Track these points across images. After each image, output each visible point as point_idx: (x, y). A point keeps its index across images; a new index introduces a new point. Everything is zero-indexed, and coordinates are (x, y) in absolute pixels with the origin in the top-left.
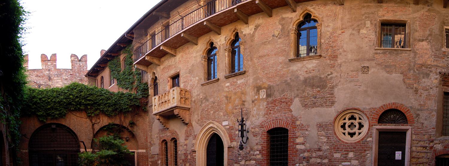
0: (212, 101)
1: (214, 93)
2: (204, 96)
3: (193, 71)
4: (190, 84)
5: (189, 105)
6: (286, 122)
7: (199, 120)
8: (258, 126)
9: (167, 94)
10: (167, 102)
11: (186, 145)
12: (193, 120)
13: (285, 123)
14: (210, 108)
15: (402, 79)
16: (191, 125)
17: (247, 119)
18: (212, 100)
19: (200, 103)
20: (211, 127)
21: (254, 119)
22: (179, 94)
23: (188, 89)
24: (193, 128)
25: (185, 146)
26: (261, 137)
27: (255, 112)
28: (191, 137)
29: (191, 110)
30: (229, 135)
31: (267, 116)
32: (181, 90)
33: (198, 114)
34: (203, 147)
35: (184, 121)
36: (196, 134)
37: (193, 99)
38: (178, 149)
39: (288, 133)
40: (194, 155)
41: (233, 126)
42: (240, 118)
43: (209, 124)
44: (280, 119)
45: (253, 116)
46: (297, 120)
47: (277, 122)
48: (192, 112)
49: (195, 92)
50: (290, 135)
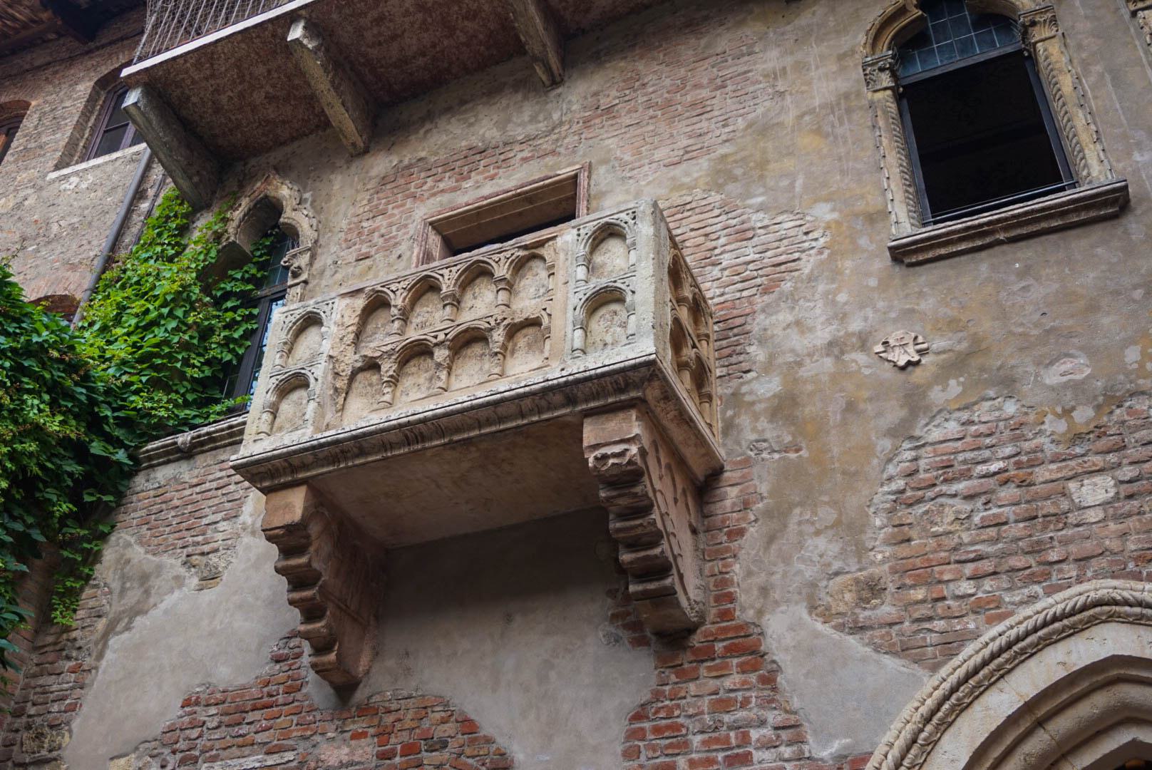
0: (1077, 387)
1: (1093, 308)
2: (938, 344)
3: (763, 164)
4: (727, 260)
7: (871, 590)
10: (498, 336)
12: (764, 591)
14: (1050, 449)
16: (732, 651)
19: (894, 413)
24: (769, 680)
29: (733, 493)
35: (668, 581)
37: (766, 387)
43: (1075, 630)
48: (746, 506)
49: (798, 323)
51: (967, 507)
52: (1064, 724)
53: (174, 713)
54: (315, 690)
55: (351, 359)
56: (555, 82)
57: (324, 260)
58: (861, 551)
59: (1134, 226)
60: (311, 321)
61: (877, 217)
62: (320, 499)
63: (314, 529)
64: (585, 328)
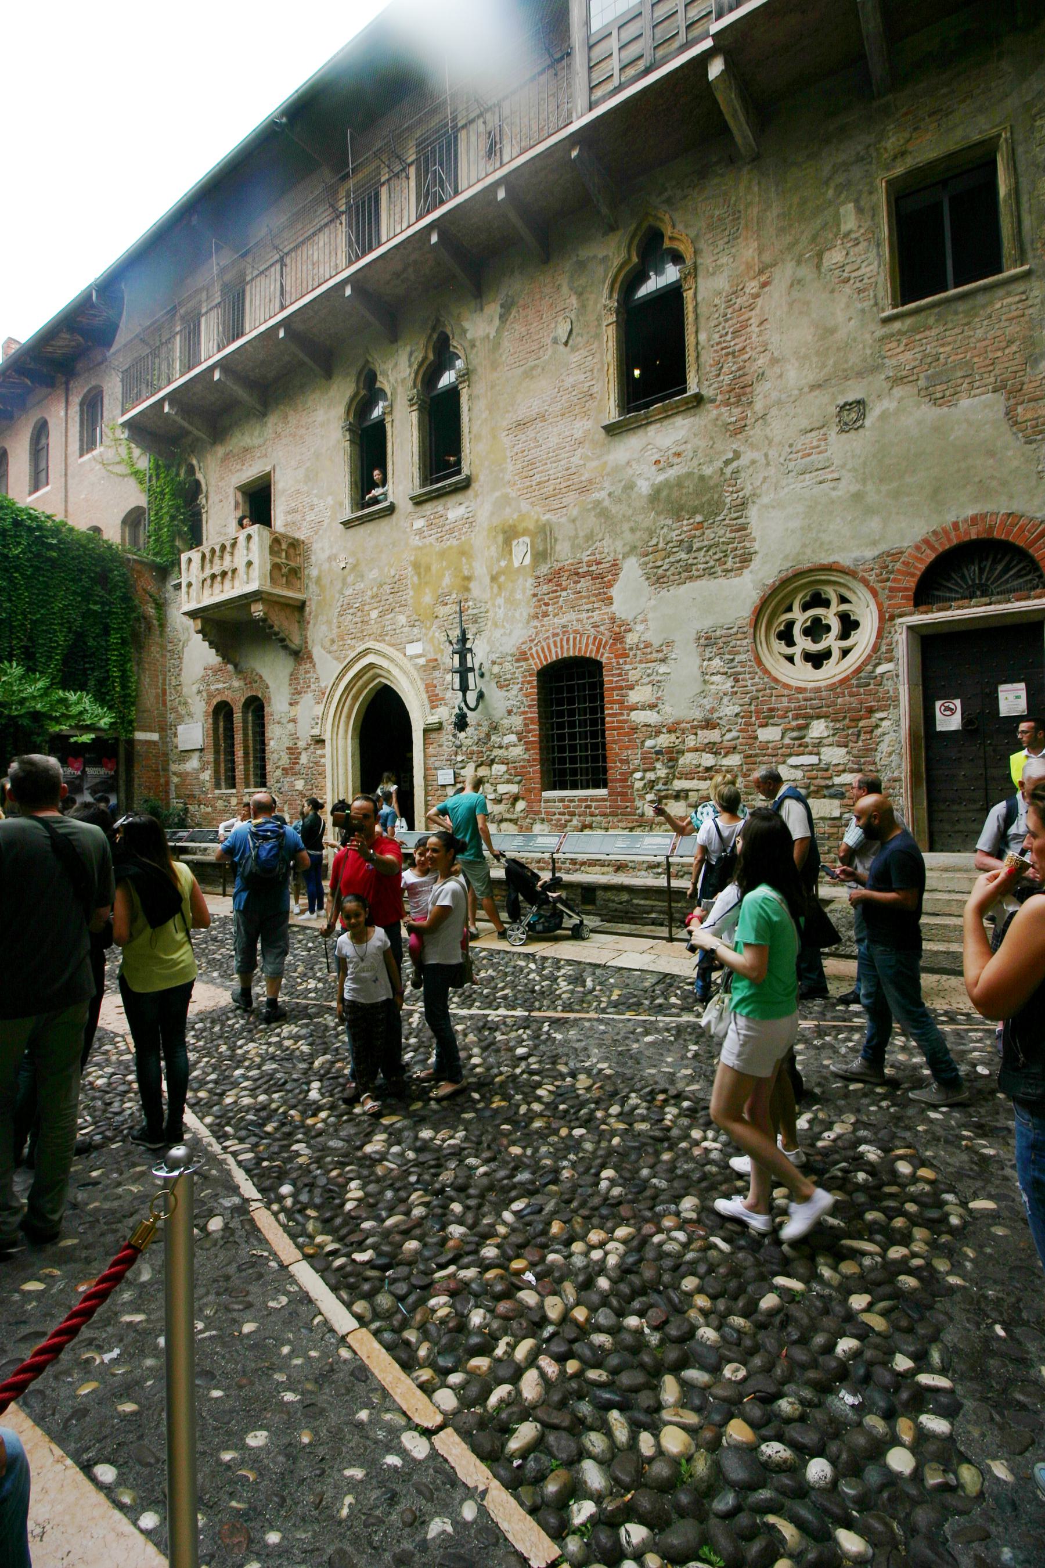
5: (299, 590)
6: (595, 638)
7: (333, 641)
8: (513, 655)
9: (228, 549)
11: (294, 721)
13: (591, 640)
15: (1001, 414)
17: (479, 632)
18: (374, 574)
19: (340, 585)
20: (371, 666)
21: (498, 633)
22: (267, 550)
23: (302, 538)
25: (292, 724)
26: (521, 689)
27: (501, 613)
28: (310, 695)
30: (427, 686)
31: (536, 623)
32: (276, 541)
33: (329, 622)
34: (346, 731)
36: (323, 685)
38: (268, 734)
39: (601, 675)
40: (319, 752)
41: (438, 657)
42: (456, 633)
44: (576, 632)
45: (496, 625)
46: (630, 630)
47: (568, 640)
49: (322, 549)
50: (609, 679)
51: (350, 617)
52: (365, 678)
53: (202, 673)
54: (230, 667)
55: (202, 576)
56: (264, 415)
57: (210, 501)
58: (331, 630)
59: (395, 516)
60: (190, 560)
61: (341, 504)
62: (206, 621)
63: (207, 629)
64: (248, 574)
